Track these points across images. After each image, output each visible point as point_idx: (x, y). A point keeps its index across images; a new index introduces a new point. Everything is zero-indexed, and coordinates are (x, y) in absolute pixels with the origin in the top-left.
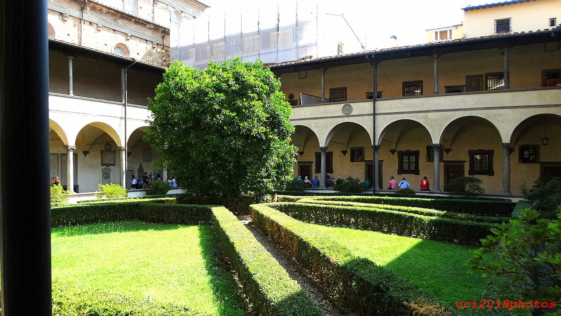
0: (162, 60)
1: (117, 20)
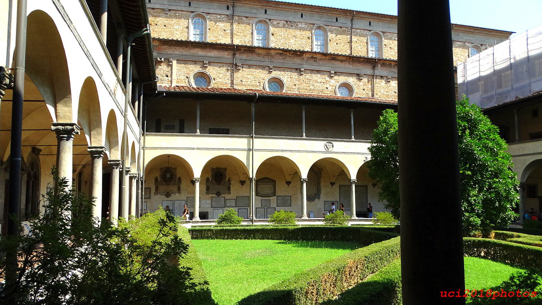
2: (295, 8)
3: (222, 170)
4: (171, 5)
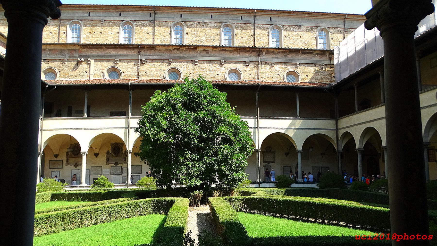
0: (330, 76)
1: (287, 55)
2: (205, 11)
3: (119, 144)
4: (105, 16)
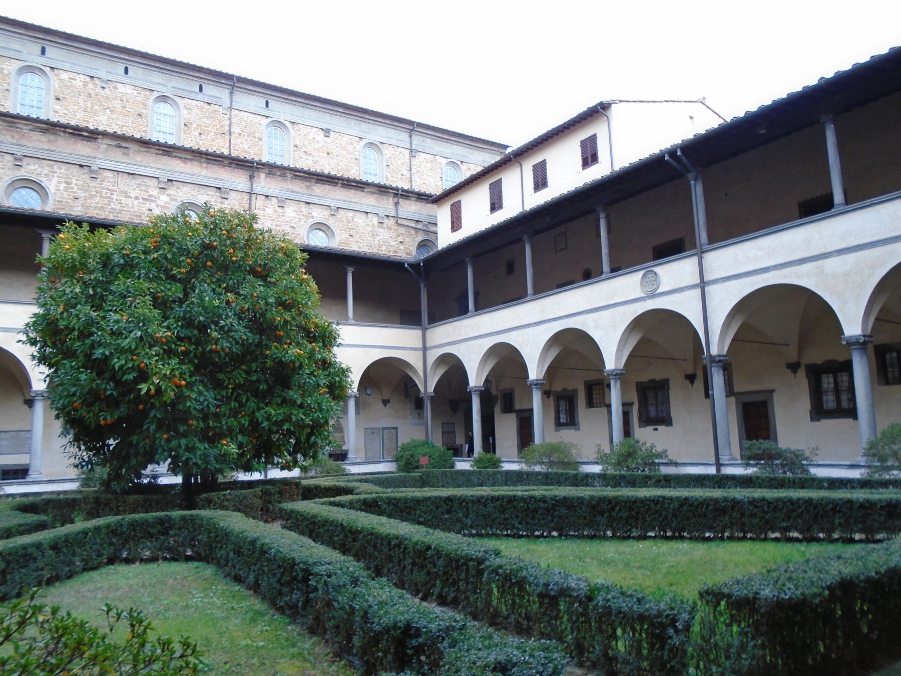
1: (313, 187)
